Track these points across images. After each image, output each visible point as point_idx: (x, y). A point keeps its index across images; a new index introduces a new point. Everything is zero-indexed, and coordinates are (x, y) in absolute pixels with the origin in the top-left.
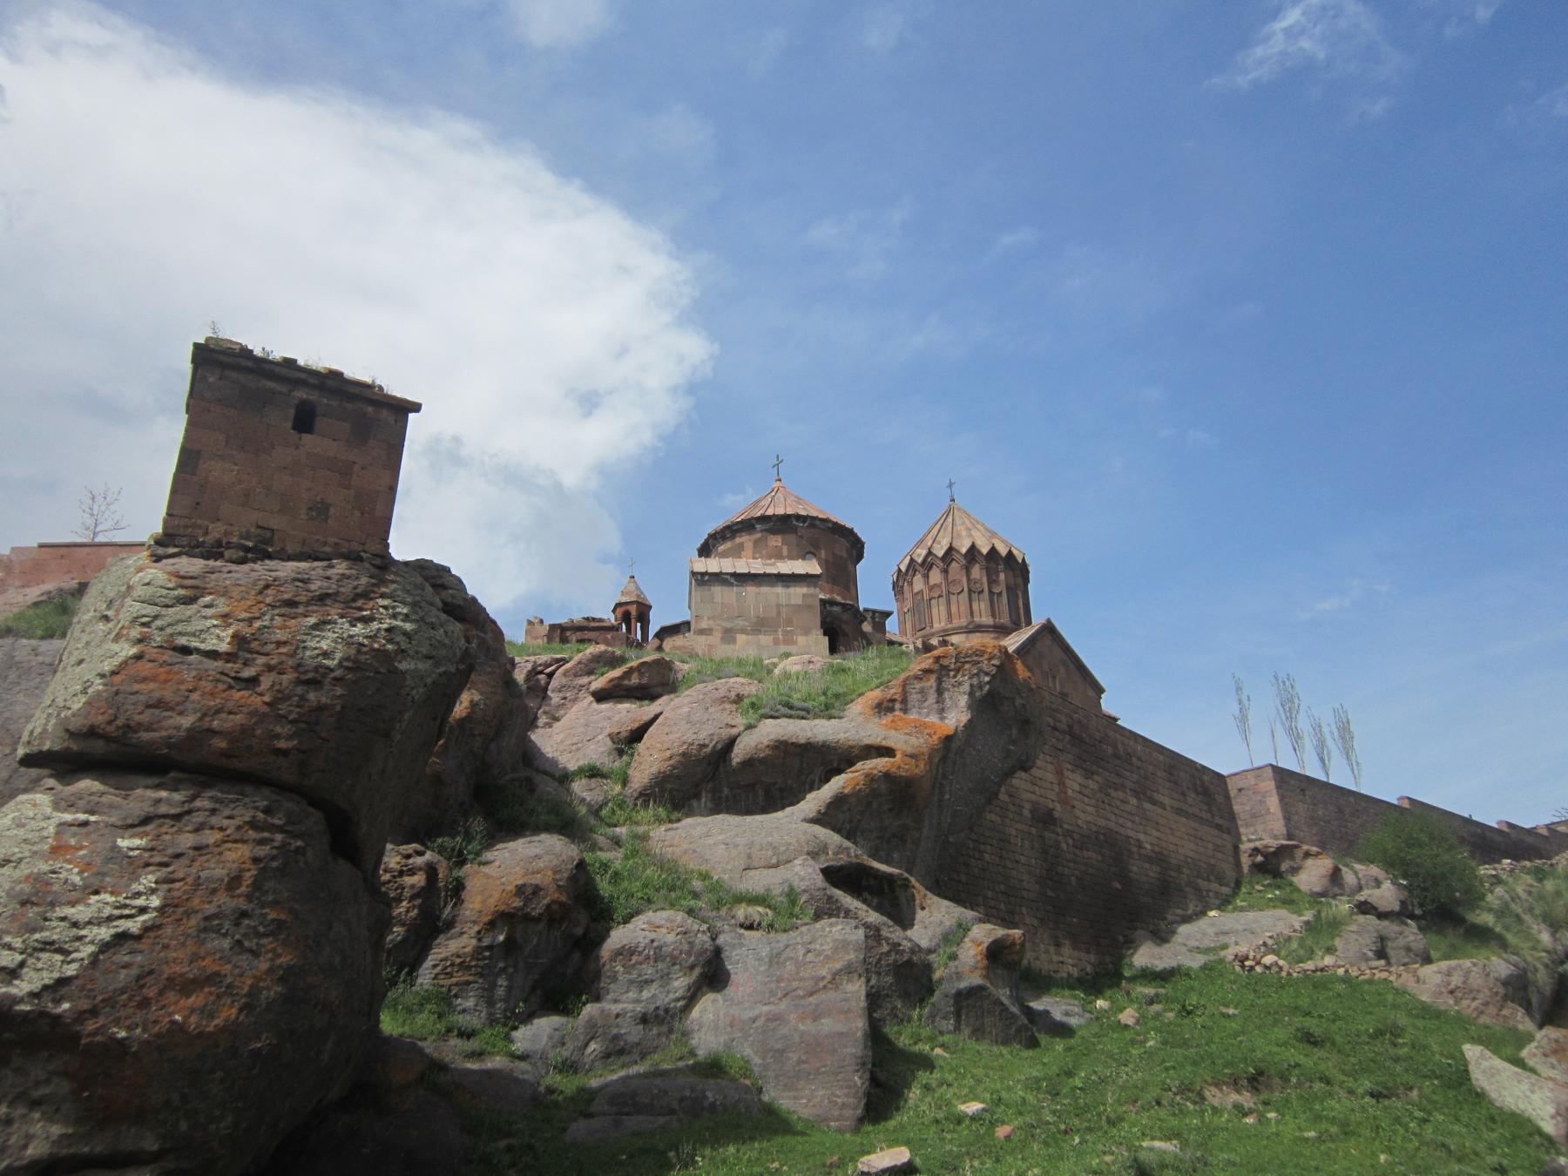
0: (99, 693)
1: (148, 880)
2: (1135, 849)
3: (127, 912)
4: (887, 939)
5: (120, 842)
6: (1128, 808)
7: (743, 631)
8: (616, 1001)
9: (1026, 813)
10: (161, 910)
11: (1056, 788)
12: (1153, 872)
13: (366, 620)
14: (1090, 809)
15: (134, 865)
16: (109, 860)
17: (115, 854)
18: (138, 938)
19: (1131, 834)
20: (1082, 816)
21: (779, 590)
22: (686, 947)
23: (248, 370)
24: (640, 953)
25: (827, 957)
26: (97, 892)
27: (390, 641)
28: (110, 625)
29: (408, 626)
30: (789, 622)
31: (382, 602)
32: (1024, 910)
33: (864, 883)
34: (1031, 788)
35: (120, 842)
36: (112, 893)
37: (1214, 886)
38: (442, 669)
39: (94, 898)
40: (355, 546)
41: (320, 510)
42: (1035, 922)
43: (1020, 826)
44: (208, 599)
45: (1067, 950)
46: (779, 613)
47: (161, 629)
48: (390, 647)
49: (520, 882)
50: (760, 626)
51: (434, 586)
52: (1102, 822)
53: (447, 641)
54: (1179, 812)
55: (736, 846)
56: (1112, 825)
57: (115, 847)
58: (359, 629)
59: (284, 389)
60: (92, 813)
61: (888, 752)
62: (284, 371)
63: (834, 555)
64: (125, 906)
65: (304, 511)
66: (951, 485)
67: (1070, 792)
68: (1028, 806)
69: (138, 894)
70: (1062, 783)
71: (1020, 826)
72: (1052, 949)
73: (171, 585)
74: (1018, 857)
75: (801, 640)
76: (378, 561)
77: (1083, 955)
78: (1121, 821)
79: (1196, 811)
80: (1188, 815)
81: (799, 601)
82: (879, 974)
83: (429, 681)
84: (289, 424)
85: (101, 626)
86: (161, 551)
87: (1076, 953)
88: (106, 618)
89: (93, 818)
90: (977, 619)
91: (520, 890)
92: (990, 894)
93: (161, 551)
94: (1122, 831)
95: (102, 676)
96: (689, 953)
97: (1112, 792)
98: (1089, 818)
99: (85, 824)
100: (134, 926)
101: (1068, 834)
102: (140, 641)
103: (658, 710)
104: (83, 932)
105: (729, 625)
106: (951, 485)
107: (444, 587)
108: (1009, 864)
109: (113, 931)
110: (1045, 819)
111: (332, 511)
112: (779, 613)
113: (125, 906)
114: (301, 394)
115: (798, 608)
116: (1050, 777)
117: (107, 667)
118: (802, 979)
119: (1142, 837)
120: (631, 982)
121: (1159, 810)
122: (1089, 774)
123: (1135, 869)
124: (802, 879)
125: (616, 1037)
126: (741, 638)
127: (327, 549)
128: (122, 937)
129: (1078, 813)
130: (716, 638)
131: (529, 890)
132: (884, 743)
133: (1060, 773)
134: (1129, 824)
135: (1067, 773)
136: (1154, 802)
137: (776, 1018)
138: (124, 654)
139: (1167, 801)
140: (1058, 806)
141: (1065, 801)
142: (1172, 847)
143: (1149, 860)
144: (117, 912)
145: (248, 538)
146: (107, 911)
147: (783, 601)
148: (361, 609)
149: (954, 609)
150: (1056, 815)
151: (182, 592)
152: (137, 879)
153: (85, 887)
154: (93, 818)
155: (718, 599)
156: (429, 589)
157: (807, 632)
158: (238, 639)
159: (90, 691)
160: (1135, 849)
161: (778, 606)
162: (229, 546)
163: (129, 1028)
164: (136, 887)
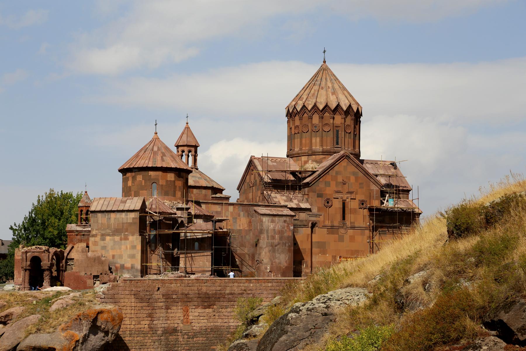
7: (109, 235)
11: (182, 318)
19: (231, 324)
20: (198, 325)
30: (127, 230)
46: (123, 226)
50: (117, 232)
52: (212, 324)
56: (219, 324)
67: (191, 317)
75: (131, 238)
78: (226, 320)
94: (226, 324)
97: (223, 310)
98: (201, 325)
105: (103, 232)
112: (123, 226)
115: (130, 224)
122: (209, 307)
126: (108, 238)
130: (98, 238)
132: (53, 347)
135: (190, 310)
140: (181, 325)
141: (186, 321)
147: (125, 221)
155: (100, 222)
157: (133, 235)
161: (123, 223)
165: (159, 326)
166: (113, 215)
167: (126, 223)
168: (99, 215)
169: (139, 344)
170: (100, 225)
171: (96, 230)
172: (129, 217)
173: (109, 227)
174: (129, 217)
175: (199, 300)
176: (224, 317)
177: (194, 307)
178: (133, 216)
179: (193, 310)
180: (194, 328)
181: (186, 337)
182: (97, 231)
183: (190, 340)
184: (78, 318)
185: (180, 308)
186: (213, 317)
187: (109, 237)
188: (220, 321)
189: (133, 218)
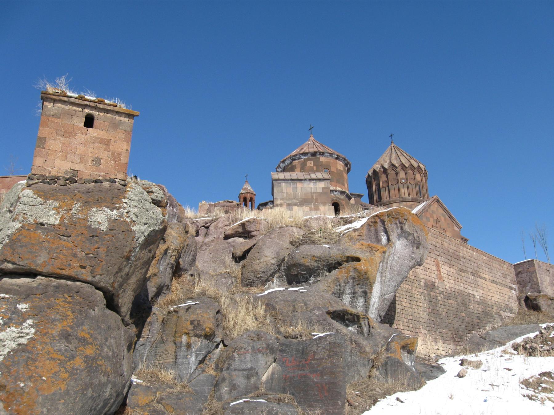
0: (7, 243)
1: (30, 322)
2: (472, 299)
3: (21, 335)
4: (355, 341)
5: (18, 306)
6: (469, 280)
7: (296, 205)
8: (235, 370)
9: (422, 284)
10: (35, 334)
11: (436, 273)
12: (480, 308)
13: (118, 208)
14: (452, 281)
15: (23, 317)
16: (13, 313)
17: (16, 311)
18: (26, 345)
19: (471, 292)
20: (448, 285)
21: (312, 185)
22: (265, 346)
23: (64, 102)
24: (245, 349)
25: (327, 350)
26: (9, 327)
27: (128, 217)
28: (12, 214)
29: (136, 210)
30: (316, 200)
31: (124, 200)
32: (421, 327)
33: (346, 317)
34: (425, 273)
35: (18, 306)
36: (16, 327)
37: (509, 314)
38: (152, 229)
39: (8, 329)
40: (113, 177)
41: (97, 161)
42: (426, 332)
43: (419, 290)
44: (50, 202)
45: (440, 344)
46: (312, 196)
47: (31, 215)
48: (128, 220)
49: (192, 320)
50: (304, 202)
51: (148, 192)
52: (457, 287)
53: (153, 216)
54: (492, 282)
55: (288, 301)
56: (462, 288)
57: (16, 308)
58: (115, 212)
59: (80, 109)
60: (6, 293)
61: (358, 259)
62: (80, 102)
63: (337, 169)
64: (21, 333)
65: (90, 162)
66: (391, 136)
67: (442, 274)
68: (423, 281)
69: (26, 328)
70: (439, 271)
71: (419, 290)
72: (433, 344)
73: (35, 197)
74: (418, 304)
75: (322, 208)
76: (122, 183)
77: (448, 346)
78: (466, 286)
79: (500, 281)
80: (496, 283)
81: (321, 191)
82: (351, 356)
83: (146, 234)
84: (83, 124)
85: (9, 215)
86: (31, 182)
87: (444, 345)
88: (10, 211)
89: (7, 296)
90: (403, 196)
91: (192, 323)
92: (405, 320)
93: (31, 182)
94: (466, 291)
95: (8, 236)
96: (267, 349)
97: (463, 274)
99: (3, 298)
100: (23, 341)
101: (441, 293)
102: (23, 221)
103: (255, 242)
104: (5, 343)
105: (289, 202)
106: (391, 136)
107: (152, 192)
108: (414, 307)
109: (16, 343)
110: (431, 286)
111: (102, 161)
112: (312, 196)
113: (21, 333)
114: (87, 111)
116: (434, 268)
117: (9, 232)
118: (317, 360)
119: (475, 293)
120: (241, 361)
121: (484, 281)
122: (451, 266)
123: (472, 307)
124: (318, 316)
125: (235, 385)
126: (295, 208)
127: (100, 178)
128: (19, 345)
129: (446, 283)
131: (196, 323)
132: (355, 255)
133: (438, 266)
134: (469, 288)
136: (482, 278)
137: (305, 376)
138: (16, 227)
139: (487, 277)
140: (437, 281)
141: (440, 278)
142: (489, 297)
143: (479, 303)
144: (18, 335)
145: (66, 175)
146: (15, 335)
147: (314, 191)
148: (115, 204)
149: (392, 192)
150: (436, 284)
151: (39, 199)
152: (25, 321)
153: (5, 324)
154: (7, 296)
155: (285, 191)
156: (145, 193)
157: (324, 204)
158: (62, 218)
159: (4, 243)
160: (472, 299)
161: (311, 193)
162: (58, 178)
163: (24, 382)
164: (25, 325)
165: (422, 276)
166: (299, 185)
167: (315, 193)
168: (284, 184)
169: (409, 294)
170: (285, 196)
171: (281, 200)
172: (317, 186)
173: (295, 197)
174: (317, 186)
175: (445, 256)
176: (464, 282)
177: (442, 263)
178: (323, 186)
179: (443, 267)
180: (447, 287)
181: (442, 296)
182: (282, 201)
183: (446, 301)
184: (378, 220)
185: (433, 259)
186: (457, 280)
187: (296, 207)
188: (462, 285)
189: (323, 188)
